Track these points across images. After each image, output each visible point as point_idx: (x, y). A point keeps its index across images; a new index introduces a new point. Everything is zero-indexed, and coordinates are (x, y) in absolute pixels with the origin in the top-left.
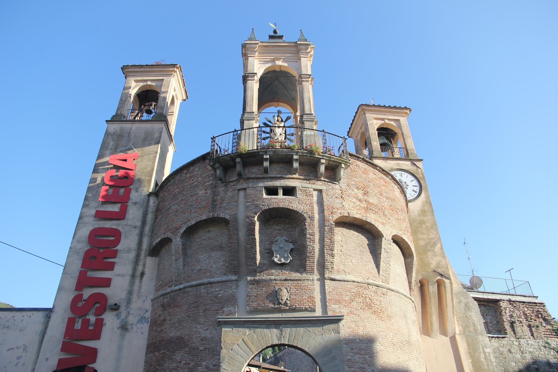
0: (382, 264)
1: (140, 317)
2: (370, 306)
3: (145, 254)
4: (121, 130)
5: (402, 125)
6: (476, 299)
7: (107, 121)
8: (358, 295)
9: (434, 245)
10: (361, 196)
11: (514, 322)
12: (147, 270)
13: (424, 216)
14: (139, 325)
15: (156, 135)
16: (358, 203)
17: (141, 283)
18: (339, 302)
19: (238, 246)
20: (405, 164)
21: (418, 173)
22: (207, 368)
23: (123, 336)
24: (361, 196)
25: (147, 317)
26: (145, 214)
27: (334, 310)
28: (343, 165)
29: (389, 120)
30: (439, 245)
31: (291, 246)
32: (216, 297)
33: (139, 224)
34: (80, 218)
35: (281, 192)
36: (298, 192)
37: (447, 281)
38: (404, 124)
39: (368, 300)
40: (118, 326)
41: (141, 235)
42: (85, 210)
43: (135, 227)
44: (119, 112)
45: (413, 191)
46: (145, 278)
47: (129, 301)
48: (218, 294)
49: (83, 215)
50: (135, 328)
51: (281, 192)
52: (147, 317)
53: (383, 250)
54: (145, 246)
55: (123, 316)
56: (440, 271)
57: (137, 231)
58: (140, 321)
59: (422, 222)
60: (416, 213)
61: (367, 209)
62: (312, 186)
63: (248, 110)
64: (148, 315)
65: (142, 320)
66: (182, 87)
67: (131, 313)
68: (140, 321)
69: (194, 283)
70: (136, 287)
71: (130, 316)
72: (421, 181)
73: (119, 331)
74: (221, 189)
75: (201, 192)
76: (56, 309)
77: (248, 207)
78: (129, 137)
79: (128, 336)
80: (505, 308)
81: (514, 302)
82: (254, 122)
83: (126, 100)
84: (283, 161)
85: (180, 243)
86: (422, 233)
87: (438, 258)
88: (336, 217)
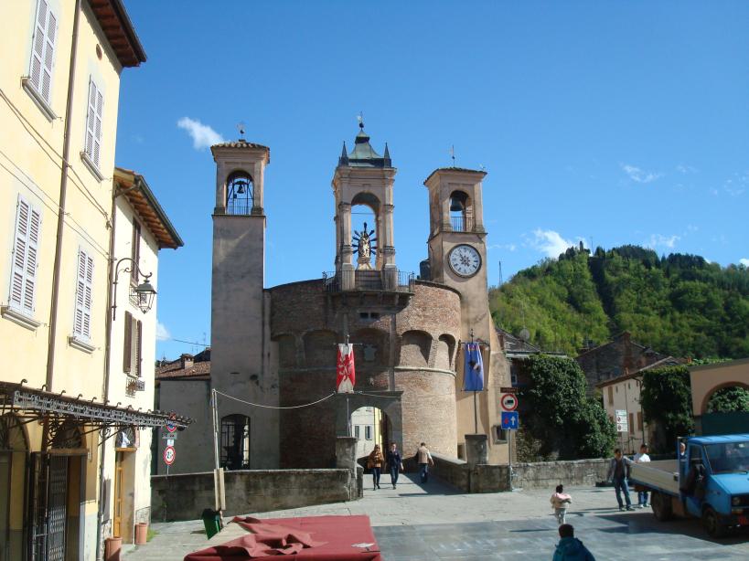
0: (430, 358)
10: (421, 313)
24: (421, 313)
26: (263, 308)
27: (399, 387)
29: (464, 184)
31: (375, 350)
33: (260, 315)
34: (213, 310)
37: (487, 349)
47: (263, 373)
57: (259, 322)
61: (423, 322)
64: (277, 382)
69: (315, 369)
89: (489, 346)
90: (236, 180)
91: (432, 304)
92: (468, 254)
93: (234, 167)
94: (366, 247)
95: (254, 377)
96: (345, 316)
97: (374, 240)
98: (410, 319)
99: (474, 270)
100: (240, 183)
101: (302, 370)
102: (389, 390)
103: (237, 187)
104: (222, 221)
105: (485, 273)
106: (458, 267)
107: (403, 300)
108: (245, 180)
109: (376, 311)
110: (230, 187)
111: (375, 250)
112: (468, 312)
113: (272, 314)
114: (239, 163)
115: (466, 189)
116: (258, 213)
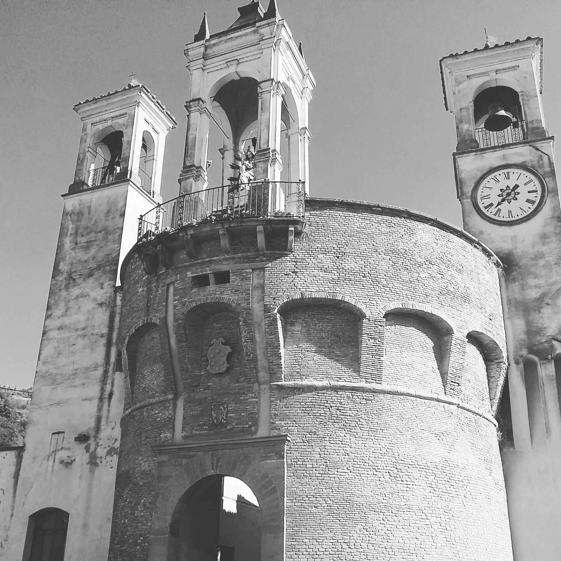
1: (109, 449)
2: (336, 420)
3: (113, 369)
4: (80, 205)
7: (63, 196)
12: (115, 389)
13: (544, 244)
14: (109, 458)
15: (121, 204)
17: (109, 406)
19: (171, 356)
20: (517, 154)
21: (541, 166)
22: (144, 506)
23: (92, 471)
25: (116, 448)
31: (228, 349)
32: (155, 420)
33: (105, 331)
38: (525, 73)
40: (87, 461)
41: (108, 346)
42: (48, 322)
43: (102, 336)
44: (77, 179)
45: (528, 201)
47: (98, 429)
48: (158, 417)
49: (47, 329)
50: (104, 462)
51: (212, 279)
52: (116, 448)
57: (104, 341)
58: (109, 453)
59: (540, 256)
64: (117, 445)
66: (160, 113)
67: (100, 444)
68: (109, 453)
69: (138, 405)
70: (104, 413)
71: (99, 448)
73: (89, 466)
76: (28, 447)
79: (97, 472)
82: (191, 180)
83: (84, 159)
86: (536, 276)
95: (82, 438)
96: (171, 289)
98: (302, 275)
99: (529, 208)
107: (279, 236)
109: (224, 267)
114: (104, 118)
115: (508, 80)
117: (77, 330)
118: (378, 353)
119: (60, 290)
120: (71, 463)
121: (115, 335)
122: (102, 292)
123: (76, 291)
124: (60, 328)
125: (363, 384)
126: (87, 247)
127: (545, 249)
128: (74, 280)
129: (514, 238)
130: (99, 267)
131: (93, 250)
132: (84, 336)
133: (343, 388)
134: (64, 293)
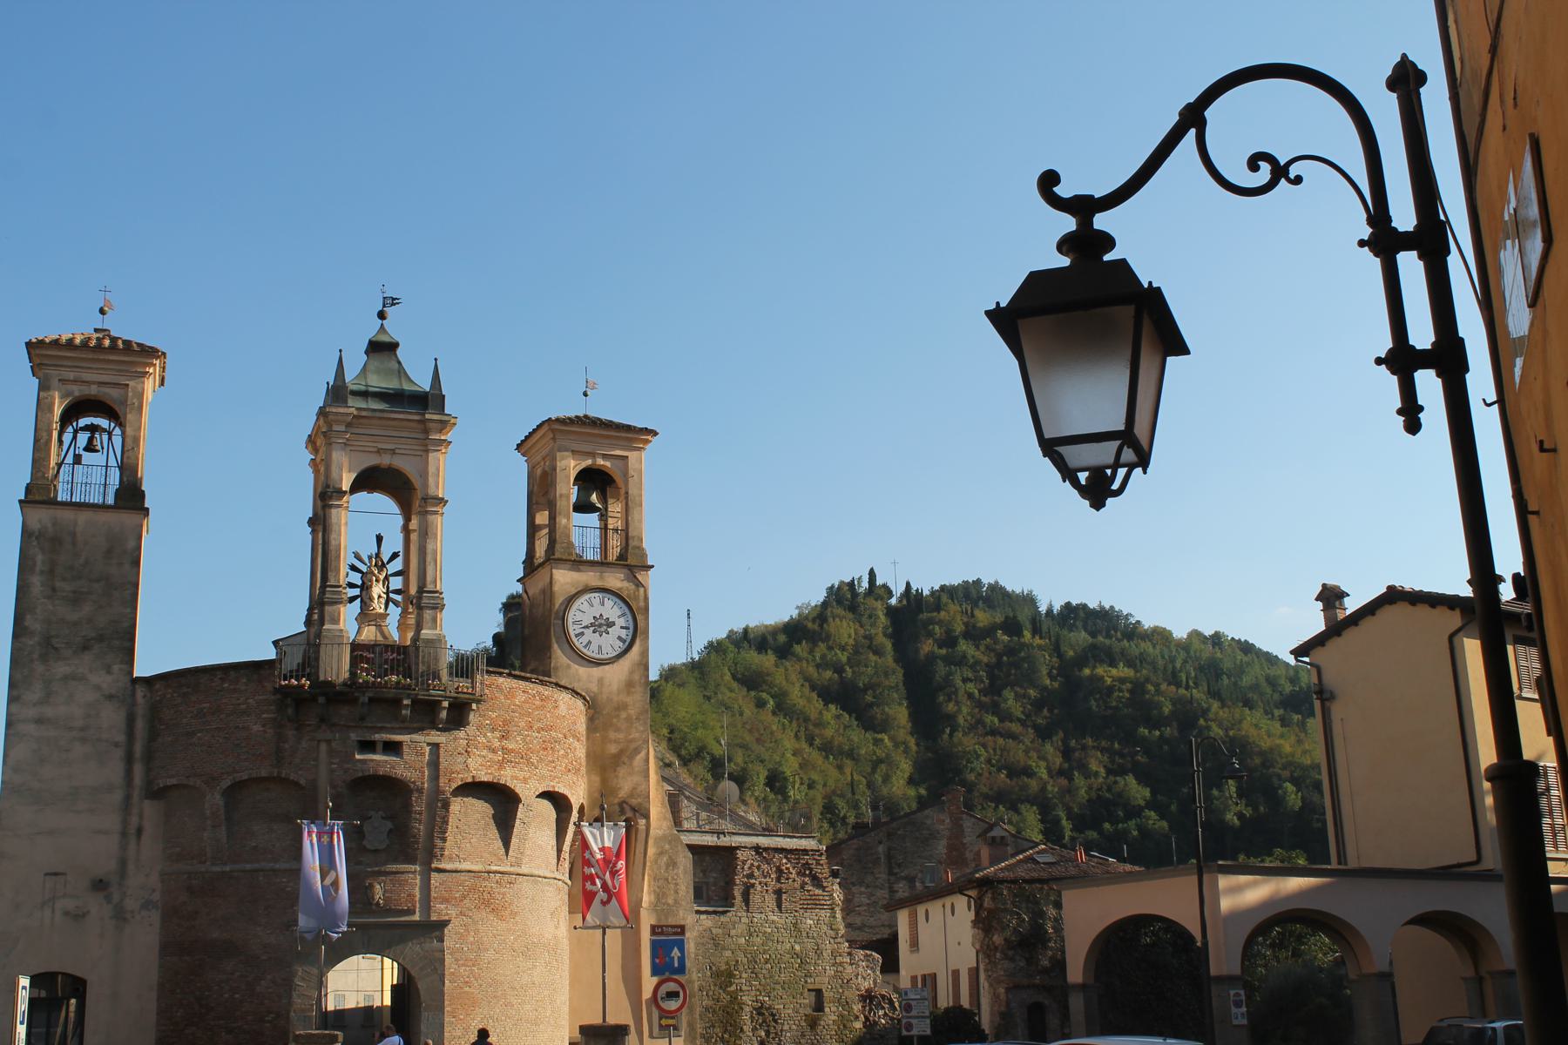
0: (514, 840)
2: (487, 903)
5: (631, 472)
6: (691, 847)
8: (473, 889)
9: (637, 751)
10: (496, 744)
11: (753, 885)
13: (629, 693)
16: (490, 756)
18: (446, 900)
21: (636, 598)
24: (496, 744)
26: (131, 720)
28: (474, 706)
30: (643, 753)
31: (389, 825)
33: (121, 738)
35: (380, 747)
36: (405, 749)
37: (642, 822)
39: (486, 896)
41: (129, 759)
42: (14, 708)
43: (116, 745)
45: (620, 638)
46: (145, 837)
51: (380, 747)
53: (518, 822)
54: (138, 780)
55: (116, 897)
56: (634, 802)
57: (119, 753)
59: (622, 707)
60: (615, 687)
62: (424, 739)
63: (332, 582)
64: (156, 896)
65: (147, 905)
69: (248, 867)
72: (639, 618)
74: (290, 733)
75: (256, 728)
77: (332, 771)
78: (74, 544)
80: (744, 862)
81: (766, 849)
84: (386, 704)
85: (221, 803)
86: (618, 730)
87: (636, 779)
88: (454, 786)
89: (647, 816)
90: (83, 422)
91: (522, 724)
92: (611, 610)
93: (78, 391)
94: (377, 590)
95: (100, 885)
96: (323, 747)
97: (396, 574)
98: (473, 753)
99: (619, 646)
100: (93, 429)
101: (217, 869)
102: (417, 917)
103: (83, 438)
104: (42, 516)
105: (645, 653)
106: (584, 640)
107: (459, 713)
108: (103, 422)
110: (67, 437)
111: (398, 598)
112: (605, 740)
113: (153, 735)
116: (131, 496)
117: (71, 729)
118: (524, 839)
119: (32, 661)
120: (84, 915)
121: (138, 748)
122: (109, 678)
123: (61, 669)
124: (39, 721)
125: (507, 869)
126: (76, 599)
127: (629, 700)
128: (56, 649)
129: (601, 681)
130: (100, 638)
131: (87, 609)
132: (84, 740)
133: (495, 872)
134: (39, 668)
